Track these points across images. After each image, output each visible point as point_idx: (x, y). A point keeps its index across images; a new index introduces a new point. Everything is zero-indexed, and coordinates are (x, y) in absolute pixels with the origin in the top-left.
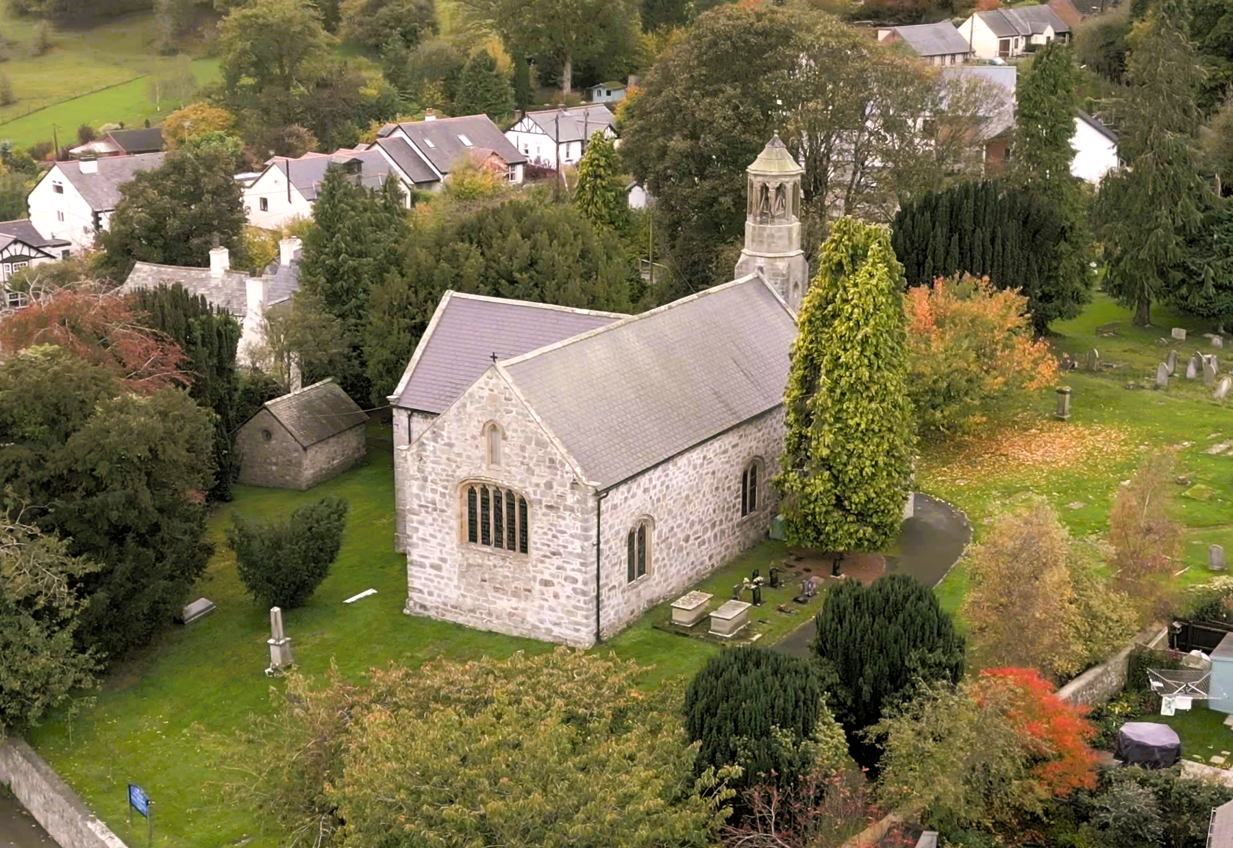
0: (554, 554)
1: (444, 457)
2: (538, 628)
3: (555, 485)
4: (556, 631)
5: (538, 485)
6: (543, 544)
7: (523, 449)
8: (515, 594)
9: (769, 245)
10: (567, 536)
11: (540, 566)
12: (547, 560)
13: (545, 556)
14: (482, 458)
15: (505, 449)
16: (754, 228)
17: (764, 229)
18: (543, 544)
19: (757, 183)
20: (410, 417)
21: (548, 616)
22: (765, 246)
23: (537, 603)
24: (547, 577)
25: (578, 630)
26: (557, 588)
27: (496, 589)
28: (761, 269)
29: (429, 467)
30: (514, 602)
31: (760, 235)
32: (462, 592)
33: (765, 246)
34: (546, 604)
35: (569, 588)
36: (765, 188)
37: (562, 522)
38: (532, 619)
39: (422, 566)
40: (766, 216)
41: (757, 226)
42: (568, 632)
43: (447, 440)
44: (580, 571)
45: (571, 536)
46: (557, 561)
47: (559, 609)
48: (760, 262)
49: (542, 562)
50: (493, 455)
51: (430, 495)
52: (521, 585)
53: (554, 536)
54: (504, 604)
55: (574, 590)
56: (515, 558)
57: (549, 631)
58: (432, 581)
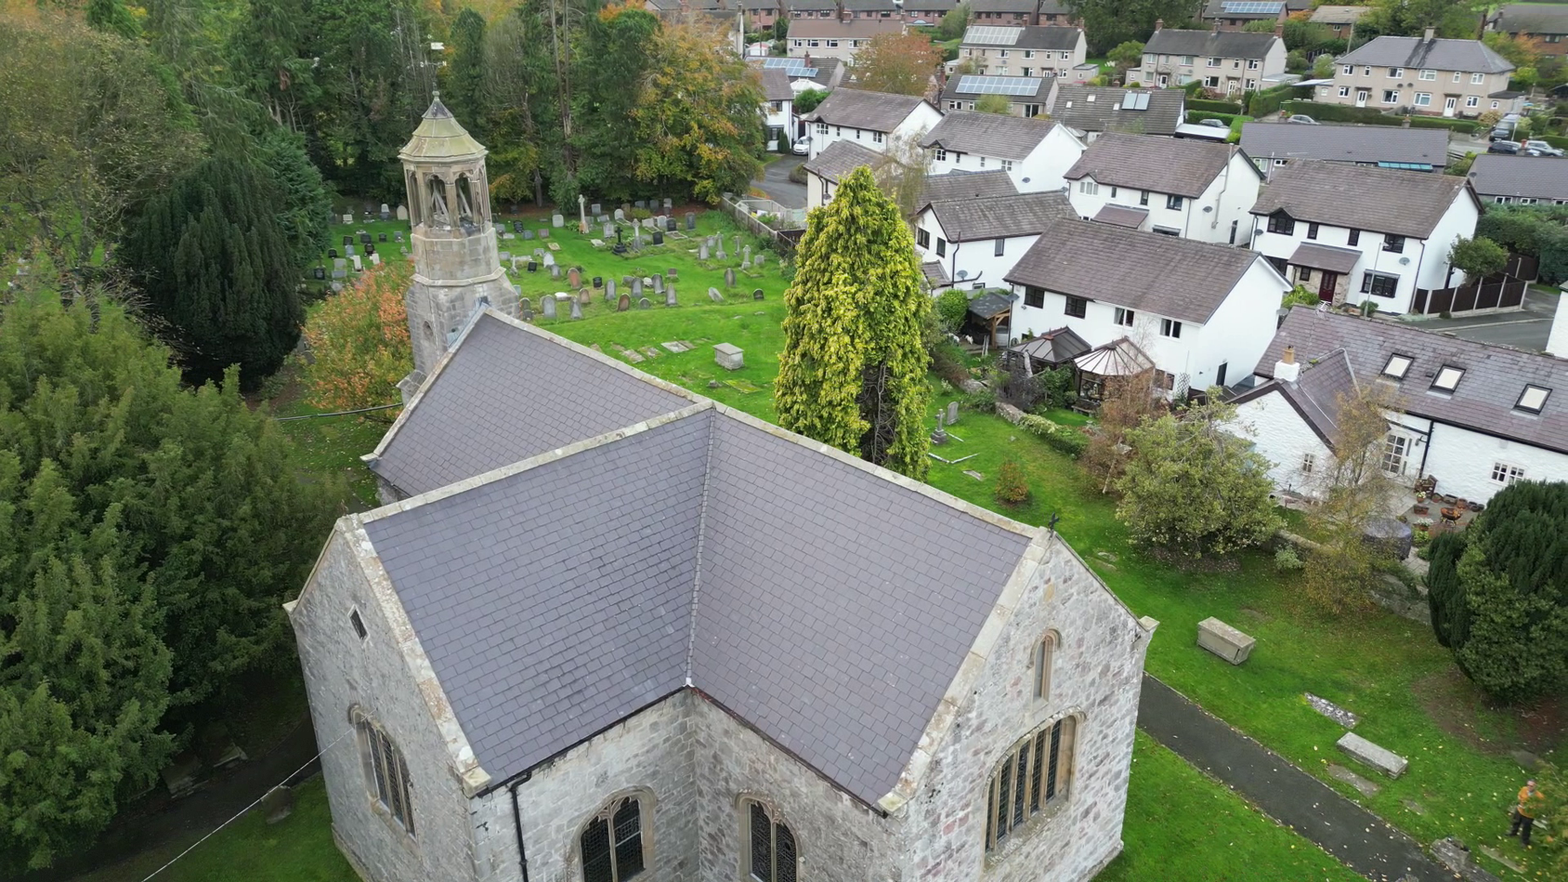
1: (969, 755)
3: (1113, 664)
4: (1090, 863)
5: (1093, 683)
7: (1080, 642)
9: (488, 264)
14: (1025, 706)
15: (1059, 661)
16: (462, 245)
17: (478, 240)
19: (450, 177)
20: (513, 791)
21: (1084, 852)
22: (483, 267)
28: (485, 300)
29: (944, 795)
31: (473, 252)
33: (483, 267)
36: (463, 183)
37: (1114, 709)
40: (467, 225)
41: (466, 240)
43: (974, 723)
46: (1103, 769)
48: (482, 291)
50: (1040, 691)
51: (940, 844)
52: (1059, 844)
55: (1117, 789)
56: (1052, 814)
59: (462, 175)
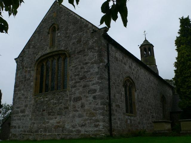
0: (81, 79)
2: (72, 131)
4: (83, 130)
6: (76, 75)
8: (60, 114)
10: (89, 64)
11: (73, 90)
12: (78, 84)
13: (76, 83)
18: (76, 75)
23: (71, 115)
24: (77, 95)
25: (96, 126)
26: (83, 101)
27: (49, 114)
30: (58, 118)
32: (33, 121)
34: (77, 114)
35: (91, 98)
38: (67, 126)
39: (18, 113)
42: (90, 129)
44: (97, 83)
45: (92, 63)
46: (82, 83)
47: (85, 114)
49: (75, 87)
53: (81, 68)
54: (53, 122)
55: (94, 98)
57: (79, 131)
58: (20, 119)
59: (145, 48)
